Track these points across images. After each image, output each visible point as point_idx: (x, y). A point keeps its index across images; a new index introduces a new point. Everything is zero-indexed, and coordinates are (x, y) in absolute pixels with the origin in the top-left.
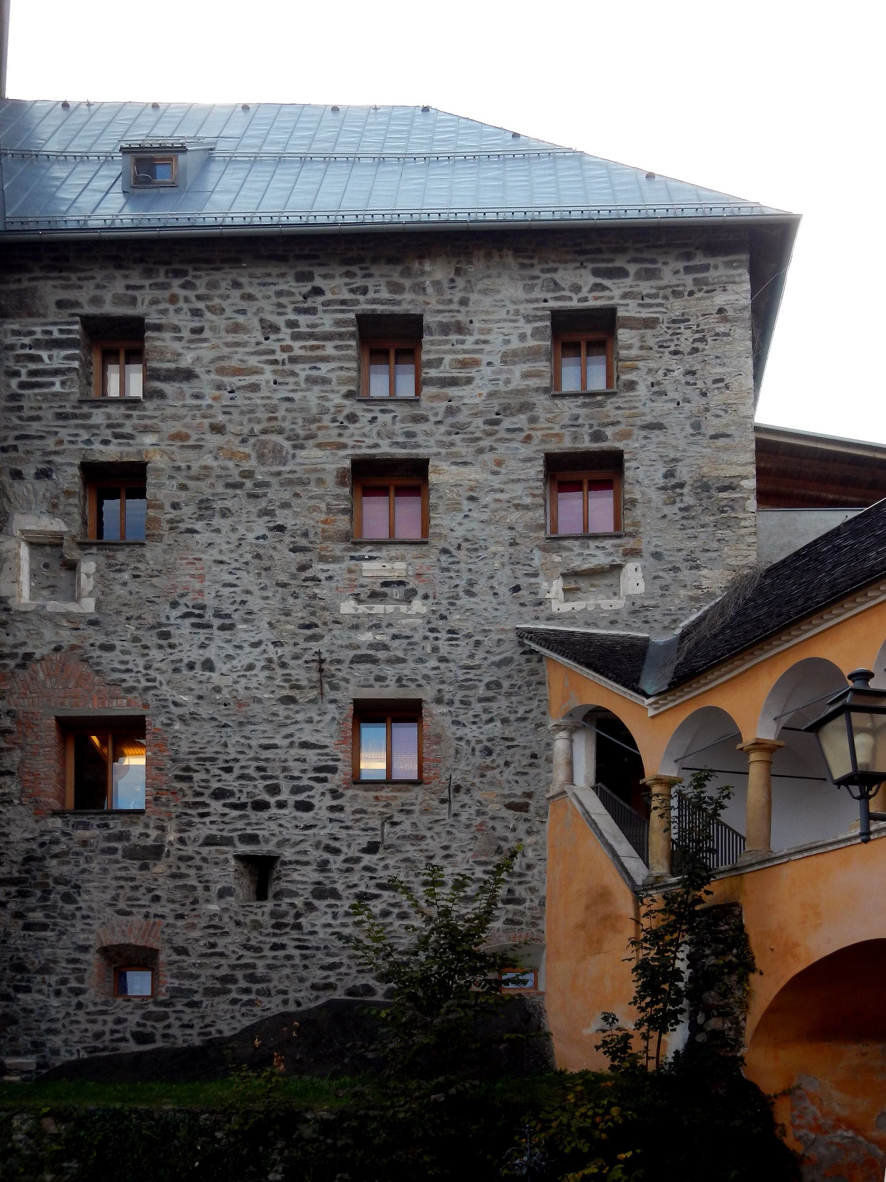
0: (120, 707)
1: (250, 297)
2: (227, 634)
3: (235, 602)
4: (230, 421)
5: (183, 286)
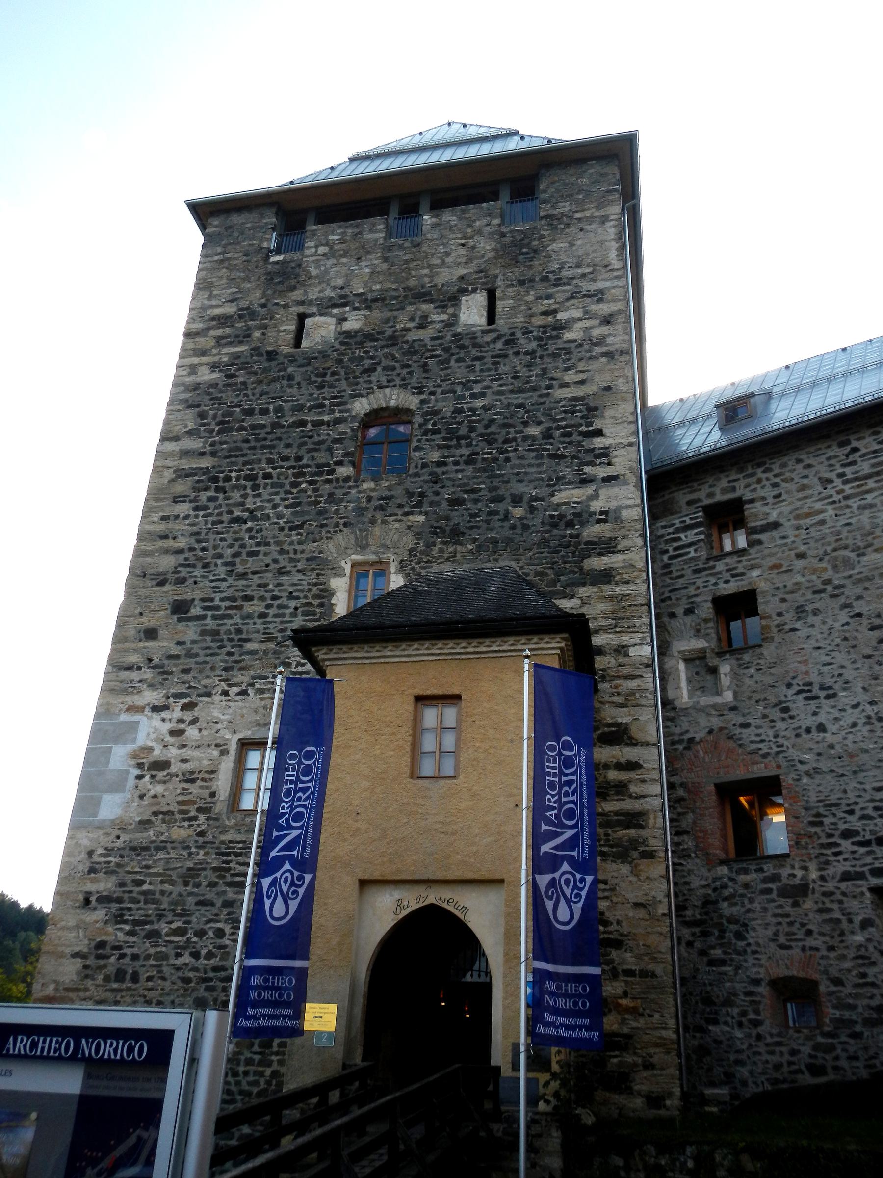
1: (809, 466)
2: (832, 702)
3: (833, 676)
4: (809, 549)
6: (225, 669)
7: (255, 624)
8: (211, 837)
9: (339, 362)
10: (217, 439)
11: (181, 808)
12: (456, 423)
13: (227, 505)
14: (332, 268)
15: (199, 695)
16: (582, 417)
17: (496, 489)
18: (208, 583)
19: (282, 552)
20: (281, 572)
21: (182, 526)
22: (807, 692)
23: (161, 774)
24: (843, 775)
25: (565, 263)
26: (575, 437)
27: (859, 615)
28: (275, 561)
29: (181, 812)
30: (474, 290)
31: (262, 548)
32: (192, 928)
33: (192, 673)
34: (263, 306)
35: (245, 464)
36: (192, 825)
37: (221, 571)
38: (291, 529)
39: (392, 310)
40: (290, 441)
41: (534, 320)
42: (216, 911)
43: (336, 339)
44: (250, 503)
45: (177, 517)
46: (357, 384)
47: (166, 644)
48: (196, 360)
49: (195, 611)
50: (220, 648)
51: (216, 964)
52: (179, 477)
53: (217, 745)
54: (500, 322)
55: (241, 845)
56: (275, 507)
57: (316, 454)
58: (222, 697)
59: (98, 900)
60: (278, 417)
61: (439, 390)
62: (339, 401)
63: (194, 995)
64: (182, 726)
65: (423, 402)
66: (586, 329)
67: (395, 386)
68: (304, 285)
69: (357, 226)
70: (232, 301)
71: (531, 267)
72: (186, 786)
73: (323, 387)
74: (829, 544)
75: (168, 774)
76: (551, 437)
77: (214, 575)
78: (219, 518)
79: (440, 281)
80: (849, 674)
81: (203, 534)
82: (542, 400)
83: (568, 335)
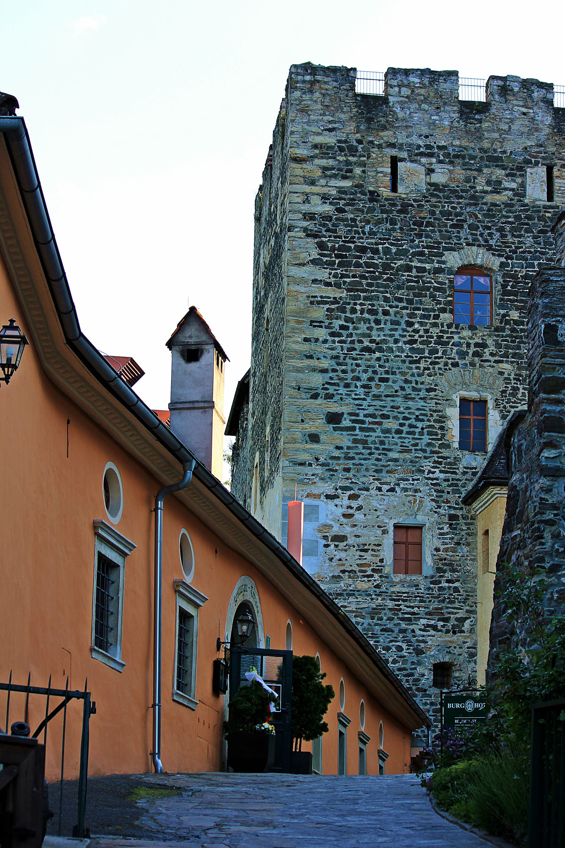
6: (376, 471)
7: (393, 438)
8: (384, 589)
9: (433, 213)
10: (339, 271)
11: (360, 568)
13: (356, 334)
15: (359, 489)
18: (352, 401)
19: (406, 381)
20: (407, 398)
21: (322, 348)
23: (342, 545)
28: (403, 388)
30: (537, 163)
31: (390, 376)
32: (380, 645)
33: (352, 472)
34: (360, 142)
35: (366, 299)
36: (371, 580)
37: (361, 391)
38: (410, 362)
45: (317, 340)
46: (450, 238)
47: (328, 447)
48: (308, 189)
49: (346, 423)
50: (370, 454)
51: (400, 667)
55: (406, 595)
56: (396, 341)
64: (351, 511)
65: (502, 265)
67: (479, 246)
68: (393, 126)
70: (330, 130)
72: (362, 554)
77: (356, 395)
78: (353, 346)
81: (342, 358)
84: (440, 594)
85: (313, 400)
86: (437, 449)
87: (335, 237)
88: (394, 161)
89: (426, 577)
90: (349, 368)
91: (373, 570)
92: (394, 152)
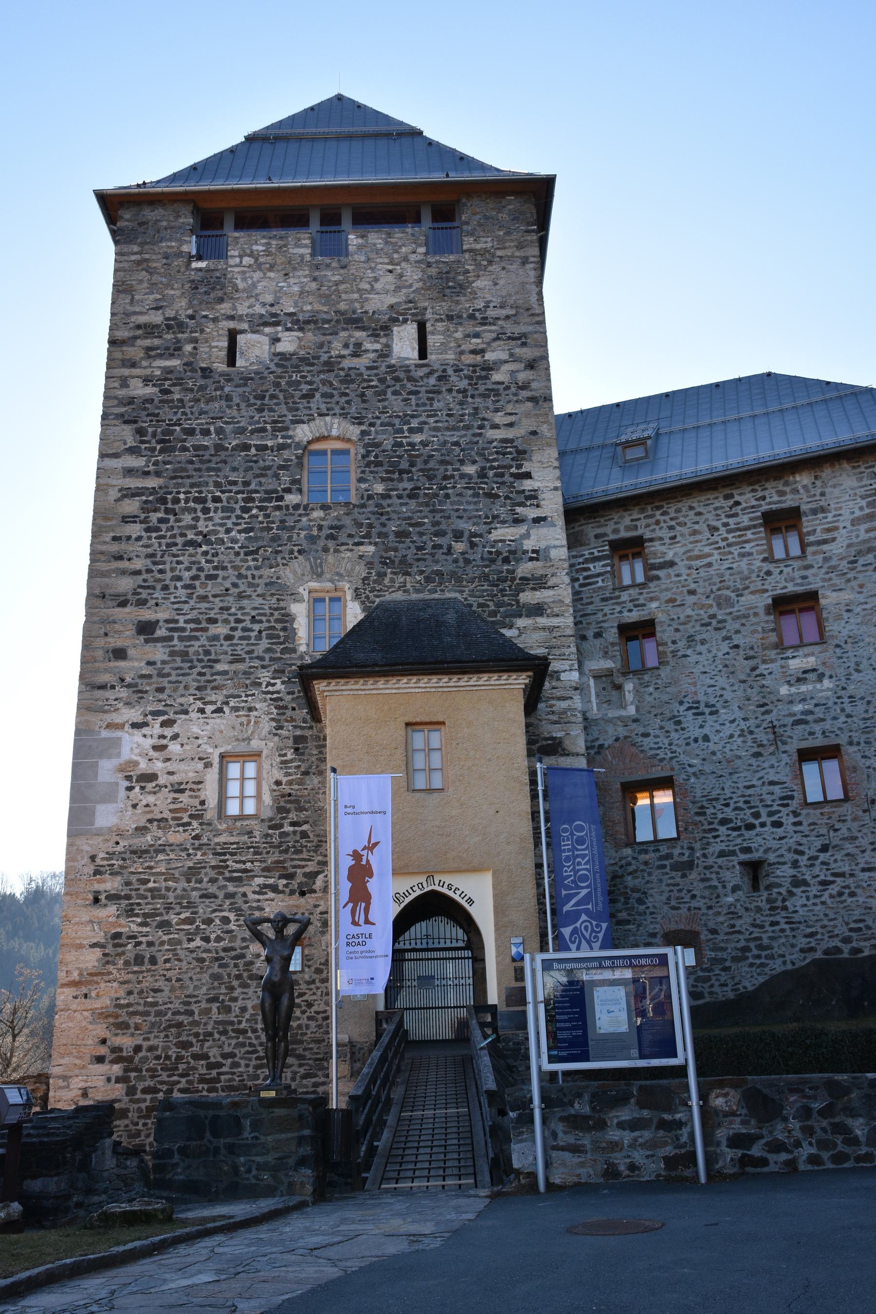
0: (657, 772)
5: (662, 514)
6: (198, 688)
7: (222, 645)
9: (277, 385)
12: (397, 457)
13: (179, 527)
14: (259, 282)
15: (176, 713)
16: (513, 459)
17: (438, 523)
19: (240, 576)
20: (241, 596)
22: (695, 708)
23: (150, 786)
24: (721, 776)
25: (490, 302)
26: (507, 478)
27: (737, 647)
28: (235, 585)
29: (174, 819)
30: (405, 321)
31: (220, 572)
33: (167, 692)
34: (192, 317)
35: (192, 485)
37: (182, 593)
38: (246, 554)
39: (325, 335)
40: (236, 464)
41: (463, 358)
42: (219, 902)
43: (272, 360)
44: (202, 526)
45: (129, 538)
46: (297, 409)
47: (136, 664)
48: (126, 372)
49: (160, 632)
50: (191, 668)
52: (124, 496)
53: (200, 759)
54: (432, 357)
56: (228, 531)
57: (263, 480)
58: (199, 715)
59: (106, 898)
60: (220, 439)
61: (378, 422)
62: (280, 427)
63: (210, 971)
64: (165, 742)
65: (363, 433)
66: (513, 372)
67: (335, 414)
68: (232, 298)
69: (281, 238)
70: (157, 308)
71: (458, 303)
72: (176, 795)
73: (263, 410)
74: (715, 584)
75: (157, 785)
76: (484, 476)
78: (173, 540)
79: (370, 308)
80: (728, 695)
82: (476, 439)
83: (497, 377)
84: (281, 842)
85: (120, 609)
86: (279, 655)
87: (158, 421)
88: (232, 336)
89: (263, 821)
90: (167, 567)
91: (191, 816)
92: (232, 324)
